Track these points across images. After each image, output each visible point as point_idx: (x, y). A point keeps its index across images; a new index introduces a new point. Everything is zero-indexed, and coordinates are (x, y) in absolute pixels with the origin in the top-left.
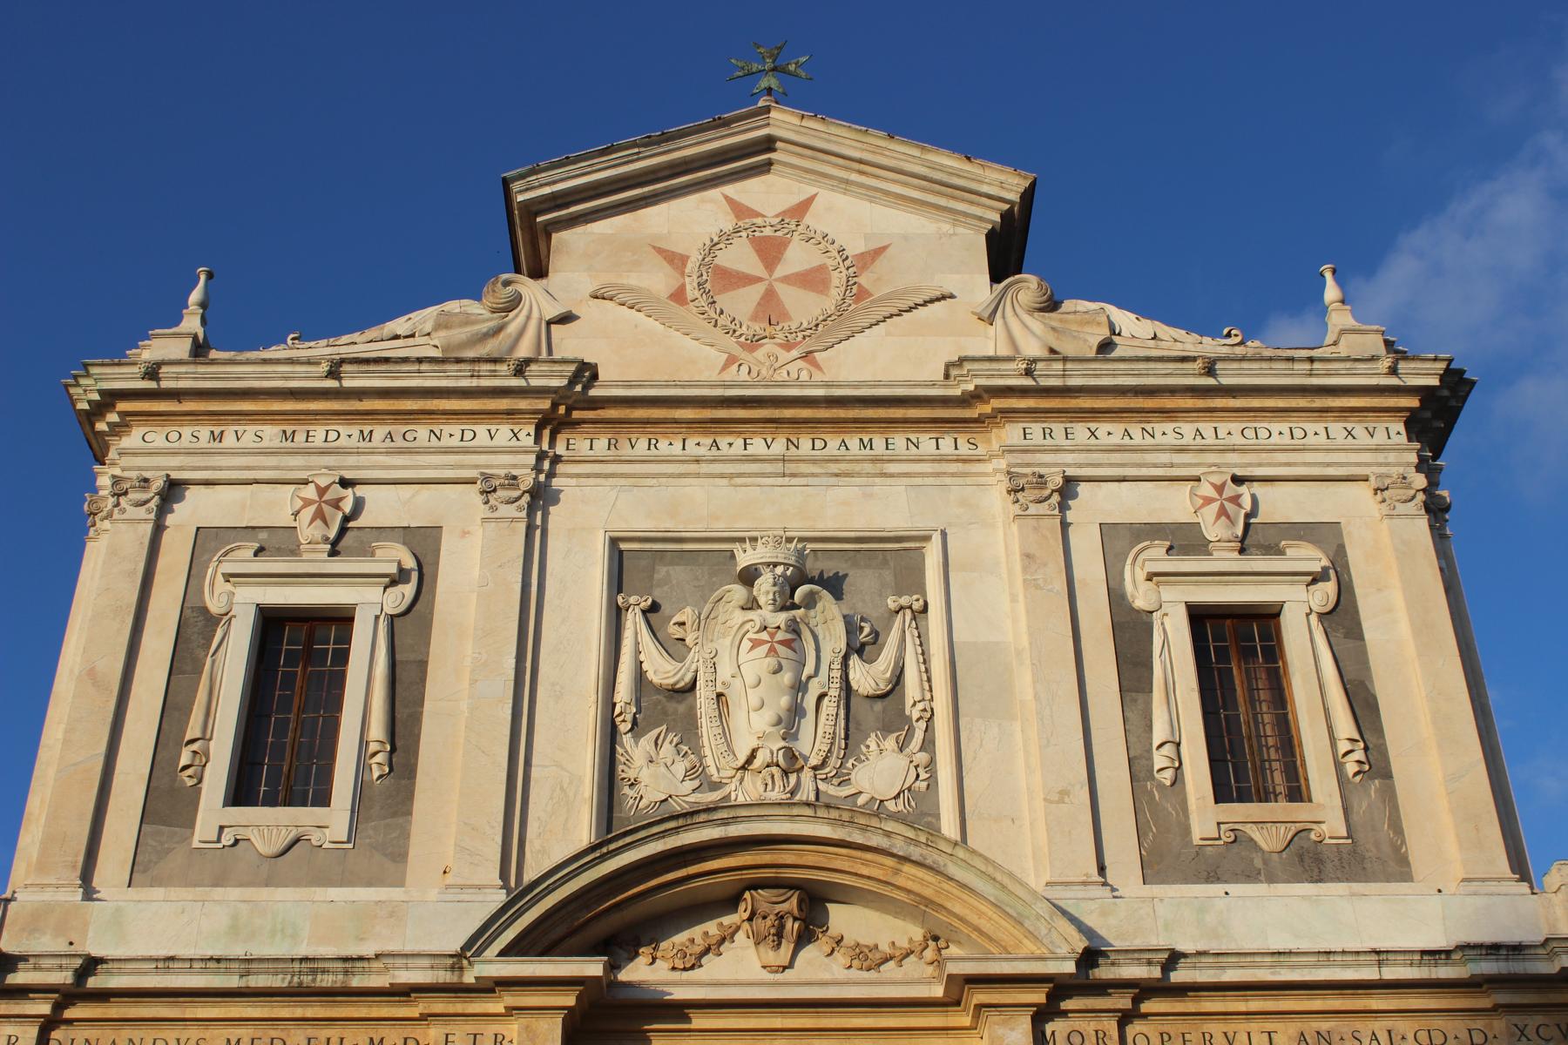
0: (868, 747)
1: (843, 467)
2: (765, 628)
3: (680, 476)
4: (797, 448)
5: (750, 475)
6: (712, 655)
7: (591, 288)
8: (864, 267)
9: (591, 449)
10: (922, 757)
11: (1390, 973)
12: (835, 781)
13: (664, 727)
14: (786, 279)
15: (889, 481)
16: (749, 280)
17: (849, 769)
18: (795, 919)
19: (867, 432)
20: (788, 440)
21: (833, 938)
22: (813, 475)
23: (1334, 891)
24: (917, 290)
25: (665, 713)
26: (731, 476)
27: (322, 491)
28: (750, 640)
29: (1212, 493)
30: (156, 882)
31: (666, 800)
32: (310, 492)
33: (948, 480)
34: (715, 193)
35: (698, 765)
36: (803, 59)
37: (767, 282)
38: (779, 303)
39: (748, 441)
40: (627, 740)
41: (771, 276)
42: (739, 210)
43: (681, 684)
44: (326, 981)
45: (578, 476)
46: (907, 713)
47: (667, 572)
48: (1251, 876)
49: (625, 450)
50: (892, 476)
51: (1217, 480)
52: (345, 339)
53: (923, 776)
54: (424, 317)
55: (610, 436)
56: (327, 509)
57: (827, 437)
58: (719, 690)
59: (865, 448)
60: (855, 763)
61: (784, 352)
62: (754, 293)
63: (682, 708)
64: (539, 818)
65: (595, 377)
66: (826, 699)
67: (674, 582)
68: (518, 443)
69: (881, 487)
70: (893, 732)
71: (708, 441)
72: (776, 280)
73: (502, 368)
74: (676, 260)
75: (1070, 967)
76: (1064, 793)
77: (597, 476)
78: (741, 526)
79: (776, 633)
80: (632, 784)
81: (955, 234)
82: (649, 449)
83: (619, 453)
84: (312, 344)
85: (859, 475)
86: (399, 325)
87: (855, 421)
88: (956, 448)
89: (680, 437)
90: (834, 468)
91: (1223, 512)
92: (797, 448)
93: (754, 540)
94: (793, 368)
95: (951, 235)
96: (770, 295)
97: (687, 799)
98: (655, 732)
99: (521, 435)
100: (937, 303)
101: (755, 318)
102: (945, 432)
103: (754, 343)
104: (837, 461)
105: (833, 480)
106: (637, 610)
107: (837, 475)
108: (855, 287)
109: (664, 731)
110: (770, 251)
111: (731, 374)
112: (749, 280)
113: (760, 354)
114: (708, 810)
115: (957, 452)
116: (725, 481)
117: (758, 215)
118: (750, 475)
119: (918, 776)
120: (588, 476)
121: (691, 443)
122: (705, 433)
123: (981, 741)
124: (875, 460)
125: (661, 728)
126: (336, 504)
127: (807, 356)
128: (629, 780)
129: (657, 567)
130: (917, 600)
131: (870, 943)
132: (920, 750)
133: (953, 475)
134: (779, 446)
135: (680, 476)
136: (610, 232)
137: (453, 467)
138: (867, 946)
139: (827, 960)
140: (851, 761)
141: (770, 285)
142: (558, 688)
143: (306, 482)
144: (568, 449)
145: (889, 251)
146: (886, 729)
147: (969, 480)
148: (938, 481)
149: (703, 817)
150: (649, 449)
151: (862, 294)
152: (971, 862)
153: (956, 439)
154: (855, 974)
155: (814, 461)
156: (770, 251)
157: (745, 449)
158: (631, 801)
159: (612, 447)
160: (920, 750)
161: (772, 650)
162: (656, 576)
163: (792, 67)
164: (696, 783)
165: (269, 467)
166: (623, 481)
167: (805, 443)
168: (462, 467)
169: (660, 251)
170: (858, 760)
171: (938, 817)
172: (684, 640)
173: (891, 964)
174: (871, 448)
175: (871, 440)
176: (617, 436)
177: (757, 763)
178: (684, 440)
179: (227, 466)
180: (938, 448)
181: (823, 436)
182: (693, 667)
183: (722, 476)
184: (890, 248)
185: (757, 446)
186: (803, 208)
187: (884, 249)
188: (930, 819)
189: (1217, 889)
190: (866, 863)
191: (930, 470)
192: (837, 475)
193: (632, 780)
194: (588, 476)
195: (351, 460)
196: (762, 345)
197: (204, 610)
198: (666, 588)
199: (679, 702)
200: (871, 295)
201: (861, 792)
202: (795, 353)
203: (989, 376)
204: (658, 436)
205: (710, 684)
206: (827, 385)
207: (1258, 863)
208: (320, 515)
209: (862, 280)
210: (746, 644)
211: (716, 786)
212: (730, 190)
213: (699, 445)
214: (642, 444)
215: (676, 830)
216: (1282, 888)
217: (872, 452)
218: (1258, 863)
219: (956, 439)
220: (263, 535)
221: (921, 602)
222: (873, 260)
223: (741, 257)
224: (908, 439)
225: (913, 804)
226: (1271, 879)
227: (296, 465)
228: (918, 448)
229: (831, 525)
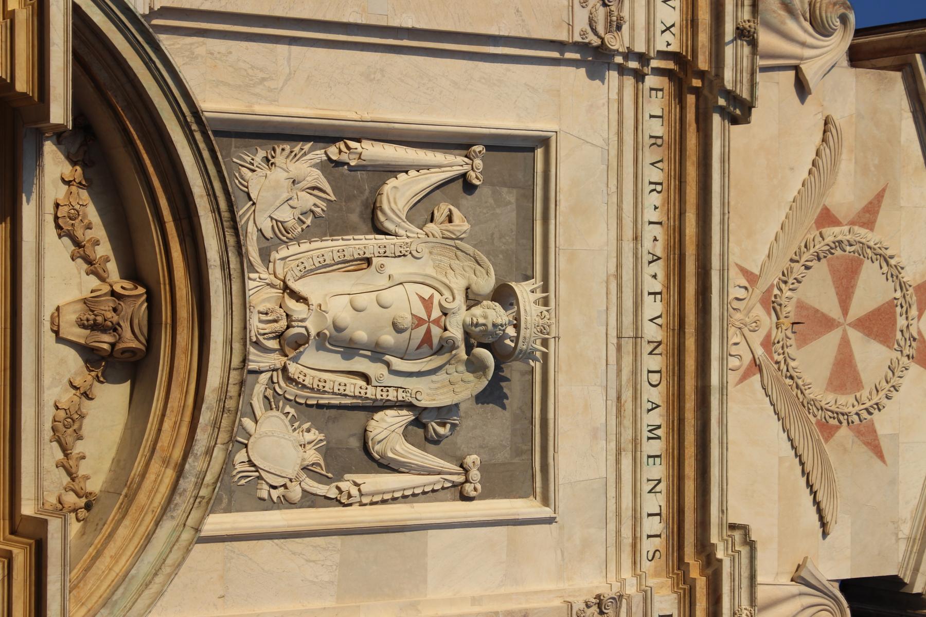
0: (308, 431)
1: (628, 406)
2: (445, 314)
3: (620, 219)
4: (651, 353)
5: (620, 298)
6: (414, 253)
7: (838, 117)
8: (859, 433)
9: (651, 116)
10: (295, 493)
12: (269, 393)
13: (333, 198)
14: (845, 343)
15: (612, 458)
16: (845, 299)
17: (283, 408)
18: (113, 345)
19: (668, 433)
20: (660, 343)
21: (91, 388)
22: (619, 371)
24: (832, 494)
25: (349, 199)
26: (619, 277)
28: (432, 297)
31: (250, 199)
33: (612, 526)
35: (289, 236)
37: (842, 320)
38: (819, 335)
39: (658, 297)
40: (319, 155)
41: (849, 325)
43: (381, 217)
45: (620, 101)
46: (347, 476)
47: (509, 203)
50: (618, 462)
53: (275, 494)
55: (666, 138)
57: (662, 387)
58: (375, 260)
59: (650, 431)
60: (290, 416)
61: (761, 339)
62: (829, 305)
63: (354, 218)
64: (230, 53)
65: (735, 121)
66: (364, 384)
67: (498, 211)
68: (658, 32)
69: (604, 450)
70: (325, 460)
71: (659, 252)
72: (845, 331)
73: (746, 14)
77: (620, 123)
78: (562, 288)
79: (439, 326)
80: (268, 160)
81: (898, 539)
82: (651, 183)
83: (646, 149)
85: (619, 424)
87: (681, 421)
88: (649, 536)
89: (664, 219)
90: (627, 395)
92: (651, 353)
93: (546, 302)
94: (743, 350)
95: (897, 535)
96: (827, 324)
97: (251, 223)
98: (328, 188)
99: (668, 36)
100: (816, 517)
101: (801, 306)
102: (667, 524)
103: (772, 304)
104: (635, 398)
105: (613, 394)
106: (467, 168)
107: (619, 398)
108: (836, 422)
109: (328, 197)
111: (734, 276)
112: (845, 299)
114: (239, 246)
115: (645, 537)
116: (612, 269)
118: (620, 298)
119: (275, 488)
120: (620, 112)
121: (657, 231)
122: (668, 248)
123: (314, 561)
124: (636, 443)
125: (332, 194)
127: (756, 366)
128: (273, 157)
129: (515, 191)
130: (475, 489)
131: (85, 431)
132: (304, 491)
133: (618, 532)
134: (652, 332)
135: (620, 219)
136: (903, 139)
138: (80, 428)
139: (65, 381)
140: (292, 411)
141: (839, 324)
142: (379, 76)
144: (651, 89)
146: (328, 452)
147: (612, 550)
148: (611, 515)
149: (231, 240)
150: (651, 183)
151: (828, 430)
152: (176, 547)
153: (659, 536)
154: (49, 413)
155: (635, 372)
157: (650, 294)
158: (249, 159)
159: (653, 141)
160: (304, 491)
161: (419, 322)
162: (505, 190)
164: (269, 234)
166: (613, 152)
167: (655, 362)
169: (880, 197)
170: (293, 420)
171: (228, 510)
172: (432, 221)
173: (60, 455)
174: (649, 438)
175: (659, 438)
176: (665, 145)
177: (291, 303)
178: (660, 223)
180: (649, 515)
181: (664, 383)
182: (401, 232)
183: (619, 266)
184: (882, 464)
185: (653, 308)
187: (881, 456)
188: (225, 501)
190: (177, 426)
191: (624, 506)
192: (619, 398)
193: (273, 160)
194: (620, 112)
196: (769, 314)
198: (491, 201)
199: (361, 215)
200: (827, 440)
201: (256, 422)
202: (760, 351)
203: (732, 576)
204: (665, 193)
205: (382, 251)
206: (723, 388)
209: (844, 431)
210: (427, 292)
211: (265, 256)
214: (656, 175)
215: (216, 209)
217: (645, 439)
219: (659, 536)
221: (473, 494)
222: (867, 444)
224: (659, 481)
225: (243, 482)
228: (650, 492)
229: (562, 390)
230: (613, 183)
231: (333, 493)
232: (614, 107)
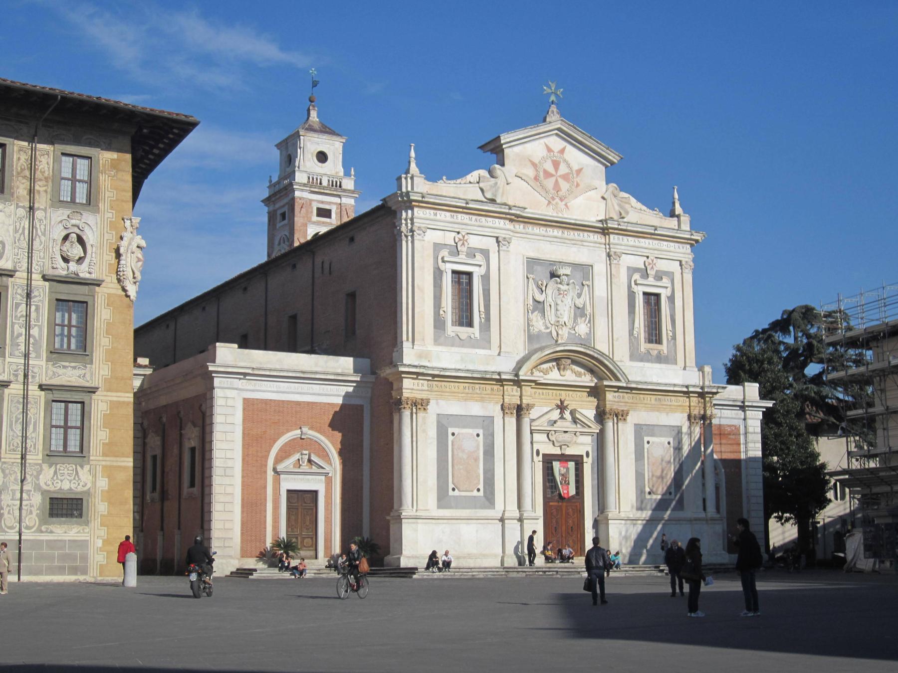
10: (589, 325)
11: (676, 389)
14: (560, 176)
16: (551, 175)
23: (663, 366)
26: (550, 241)
27: (464, 237)
29: (651, 262)
30: (439, 345)
32: (460, 236)
33: (596, 249)
34: (542, 141)
36: (562, 90)
42: (549, 150)
44: (488, 376)
45: (517, 237)
48: (648, 361)
49: (527, 230)
51: (652, 258)
52: (459, 181)
54: (474, 176)
56: (465, 242)
62: (553, 180)
63: (541, 306)
73: (507, 207)
74: (534, 165)
75: (624, 385)
76: (617, 339)
84: (449, 182)
86: (469, 177)
90: (573, 242)
91: (652, 268)
96: (557, 181)
101: (554, 189)
103: (553, 199)
110: (556, 165)
113: (554, 202)
116: (548, 243)
117: (553, 151)
124: (582, 241)
126: (466, 241)
137: (492, 232)
143: (458, 233)
145: (583, 170)
156: (556, 165)
162: (534, 269)
163: (558, 93)
165: (450, 226)
166: (527, 240)
168: (494, 233)
179: (440, 225)
186: (562, 151)
189: (641, 364)
195: (469, 227)
197: (439, 268)
202: (563, 203)
207: (650, 358)
208: (463, 244)
212: (545, 140)
213: (542, 230)
216: (654, 364)
218: (650, 358)
220: (448, 247)
223: (549, 167)
226: (652, 362)
227: (457, 228)
230: (532, 240)
231: (588, 316)
232: (519, 239)
